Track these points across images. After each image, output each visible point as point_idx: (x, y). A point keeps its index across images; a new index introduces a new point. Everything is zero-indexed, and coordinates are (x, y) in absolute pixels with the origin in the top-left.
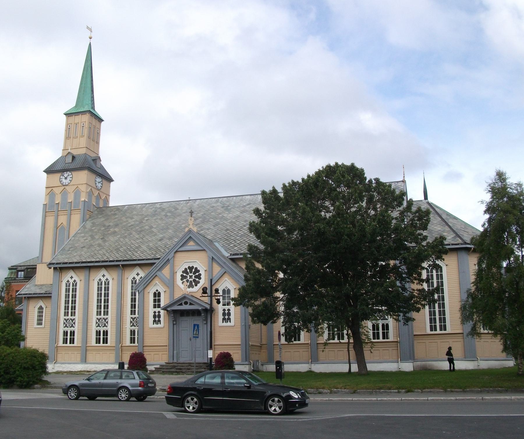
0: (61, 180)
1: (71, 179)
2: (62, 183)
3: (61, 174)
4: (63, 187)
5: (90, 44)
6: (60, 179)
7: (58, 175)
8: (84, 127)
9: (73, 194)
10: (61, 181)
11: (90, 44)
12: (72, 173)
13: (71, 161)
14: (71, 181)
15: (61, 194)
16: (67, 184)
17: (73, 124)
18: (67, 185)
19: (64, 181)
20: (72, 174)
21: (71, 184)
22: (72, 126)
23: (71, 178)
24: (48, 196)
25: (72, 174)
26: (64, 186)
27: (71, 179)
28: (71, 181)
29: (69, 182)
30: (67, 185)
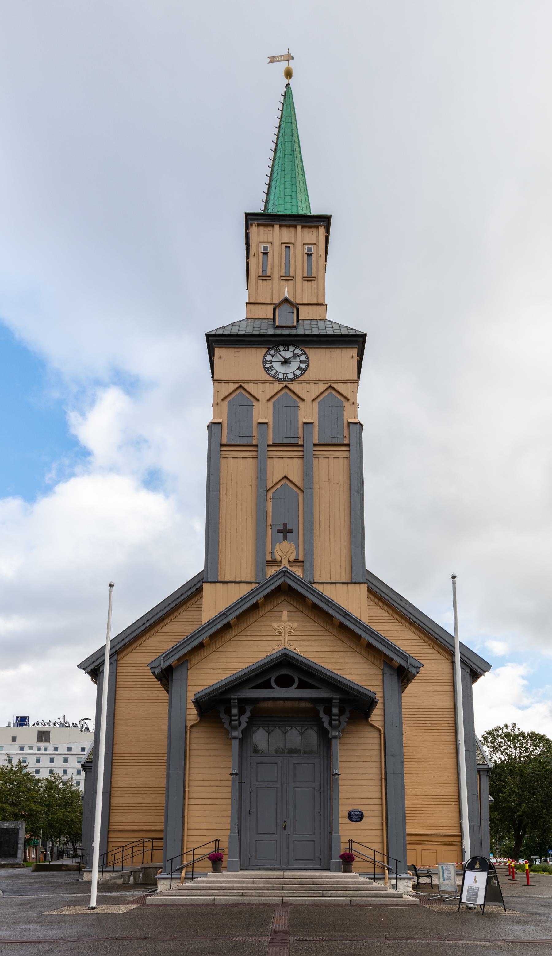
0: (268, 366)
1: (303, 366)
2: (273, 372)
6: (264, 362)
8: (314, 256)
10: (267, 370)
12: (307, 350)
14: (303, 371)
15: (271, 403)
16: (291, 376)
17: (277, 243)
18: (292, 380)
19: (278, 368)
20: (304, 353)
25: (304, 353)
28: (299, 368)
29: (298, 372)
30: (292, 380)
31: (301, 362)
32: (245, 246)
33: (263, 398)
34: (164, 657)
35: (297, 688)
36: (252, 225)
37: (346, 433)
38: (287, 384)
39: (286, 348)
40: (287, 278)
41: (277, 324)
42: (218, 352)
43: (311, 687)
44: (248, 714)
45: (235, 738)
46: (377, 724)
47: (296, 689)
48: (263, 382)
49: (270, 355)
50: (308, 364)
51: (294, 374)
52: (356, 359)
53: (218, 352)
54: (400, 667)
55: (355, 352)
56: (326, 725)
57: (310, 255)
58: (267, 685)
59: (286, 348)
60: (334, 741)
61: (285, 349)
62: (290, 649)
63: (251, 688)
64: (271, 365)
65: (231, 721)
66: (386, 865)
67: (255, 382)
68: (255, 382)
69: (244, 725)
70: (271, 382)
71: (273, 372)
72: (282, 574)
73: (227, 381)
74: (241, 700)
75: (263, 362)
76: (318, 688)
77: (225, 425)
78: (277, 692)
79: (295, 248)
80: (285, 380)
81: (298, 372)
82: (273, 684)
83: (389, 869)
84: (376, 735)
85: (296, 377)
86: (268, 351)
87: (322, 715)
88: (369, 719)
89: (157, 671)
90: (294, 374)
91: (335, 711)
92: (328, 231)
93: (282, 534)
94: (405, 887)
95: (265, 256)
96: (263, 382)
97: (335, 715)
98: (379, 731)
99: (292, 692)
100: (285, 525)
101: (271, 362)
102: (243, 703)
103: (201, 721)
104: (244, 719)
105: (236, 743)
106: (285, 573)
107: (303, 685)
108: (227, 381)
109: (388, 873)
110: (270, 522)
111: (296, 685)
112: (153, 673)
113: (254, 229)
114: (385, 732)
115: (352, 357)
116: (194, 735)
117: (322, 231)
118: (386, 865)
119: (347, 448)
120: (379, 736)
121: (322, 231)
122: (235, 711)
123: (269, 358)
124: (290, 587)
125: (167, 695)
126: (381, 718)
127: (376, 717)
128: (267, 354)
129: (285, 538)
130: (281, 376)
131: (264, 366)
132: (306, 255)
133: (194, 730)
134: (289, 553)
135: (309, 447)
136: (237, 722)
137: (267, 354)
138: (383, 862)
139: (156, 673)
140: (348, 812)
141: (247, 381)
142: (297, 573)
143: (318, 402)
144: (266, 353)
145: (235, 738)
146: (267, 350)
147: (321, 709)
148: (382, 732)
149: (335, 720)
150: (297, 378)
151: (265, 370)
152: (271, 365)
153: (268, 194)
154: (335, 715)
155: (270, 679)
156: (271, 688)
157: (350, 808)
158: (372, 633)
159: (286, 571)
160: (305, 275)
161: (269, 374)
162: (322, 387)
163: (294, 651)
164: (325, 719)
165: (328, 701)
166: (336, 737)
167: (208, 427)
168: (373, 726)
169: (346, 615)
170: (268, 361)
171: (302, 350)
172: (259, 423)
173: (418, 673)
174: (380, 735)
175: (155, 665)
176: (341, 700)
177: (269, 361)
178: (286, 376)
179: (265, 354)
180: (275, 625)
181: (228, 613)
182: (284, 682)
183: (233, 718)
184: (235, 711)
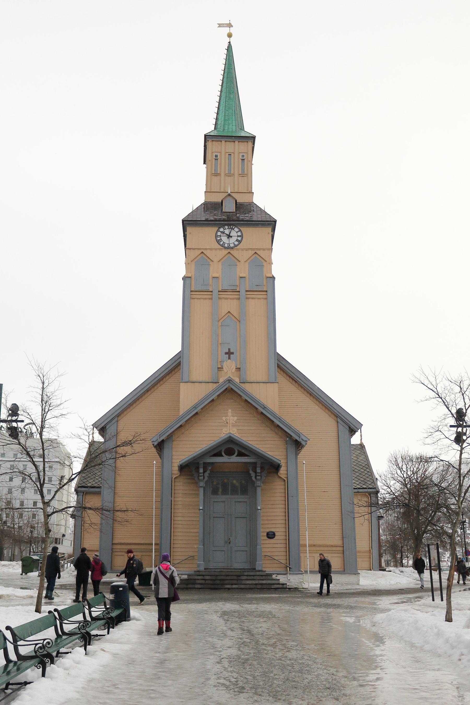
0: (218, 238)
1: (239, 239)
2: (221, 243)
3: (217, 229)
4: (227, 251)
5: (229, 49)
6: (216, 236)
7: (211, 231)
8: (245, 160)
9: (247, 264)
10: (218, 242)
11: (229, 49)
12: (241, 229)
13: (235, 211)
14: (240, 242)
16: (232, 245)
18: (232, 248)
21: (241, 246)
22: (221, 157)
23: (238, 236)
24: (193, 263)
26: (225, 248)
27: (239, 239)
28: (237, 240)
29: (236, 243)
31: (238, 236)
32: (204, 147)
33: (215, 259)
34: (160, 435)
35: (237, 456)
36: (208, 141)
37: (265, 283)
38: (230, 251)
39: (229, 227)
40: (229, 175)
41: (224, 210)
42: (189, 229)
43: (245, 455)
44: (208, 472)
45: (201, 487)
46: (283, 476)
47: (236, 456)
48: (216, 249)
49: (220, 231)
50: (242, 238)
51: (234, 244)
52: (271, 233)
53: (189, 229)
54: (296, 440)
55: (269, 229)
56: (253, 478)
57: (243, 160)
58: (218, 454)
59: (229, 227)
60: (259, 490)
61: (228, 228)
62: (233, 433)
63: (211, 456)
64: (220, 238)
65: (199, 476)
66: (288, 565)
67: (211, 249)
68: (211, 249)
69: (206, 478)
70: (220, 249)
71: (221, 243)
72: (228, 382)
73: (194, 249)
74: (204, 463)
75: (216, 236)
76: (249, 456)
77: (193, 278)
78: (225, 459)
79: (234, 155)
80: (229, 248)
81: (236, 243)
82: (223, 454)
83: (290, 568)
84: (283, 483)
85: (236, 246)
86: (218, 229)
87: (251, 472)
88: (279, 473)
89: (156, 444)
90: (234, 244)
91: (258, 470)
92: (254, 144)
93: (227, 355)
94: (299, 579)
95: (217, 160)
96: (216, 249)
97: (259, 473)
98: (285, 481)
99: (234, 459)
100: (229, 349)
101: (220, 236)
102: (206, 465)
103: (180, 475)
104: (207, 474)
105: (201, 490)
106: (230, 381)
107: (240, 454)
108: (194, 249)
109: (289, 570)
110: (220, 342)
111: (236, 454)
112: (153, 445)
113: (209, 144)
114: (287, 482)
115: (268, 233)
116: (177, 484)
117: (250, 144)
118: (288, 565)
119: (265, 293)
120: (284, 484)
121: (250, 144)
122: (201, 470)
123: (219, 234)
124: (232, 389)
125: (160, 461)
126: (285, 472)
127: (282, 471)
128: (218, 231)
129: (229, 358)
130: (226, 245)
131: (216, 239)
132: (241, 160)
133: (176, 480)
134: (232, 368)
135: (243, 292)
136: (202, 477)
137: (218, 231)
138: (287, 563)
139: (155, 445)
140: (266, 533)
141: (206, 249)
142: (236, 381)
143: (249, 263)
144: (218, 230)
145: (201, 487)
146: (217, 229)
147: (250, 469)
148: (286, 482)
149: (259, 476)
150: (236, 246)
151: (217, 241)
152: (220, 238)
153: (217, 114)
154: (259, 473)
155: (221, 450)
156: (223, 456)
157: (268, 530)
158: (280, 420)
159: (230, 380)
160: (240, 173)
161: (219, 244)
162: (251, 253)
163: (235, 434)
164: (253, 474)
165: (255, 463)
166: (259, 486)
167: (183, 278)
168: (280, 477)
169: (264, 408)
170: (218, 236)
171: (239, 228)
172: (213, 277)
173: (306, 444)
174: (285, 483)
175: (154, 439)
176: (262, 463)
177: (219, 236)
178: (229, 245)
179: (217, 231)
180: (224, 418)
181: (197, 407)
182: (230, 452)
183: (201, 475)
184: (201, 470)
